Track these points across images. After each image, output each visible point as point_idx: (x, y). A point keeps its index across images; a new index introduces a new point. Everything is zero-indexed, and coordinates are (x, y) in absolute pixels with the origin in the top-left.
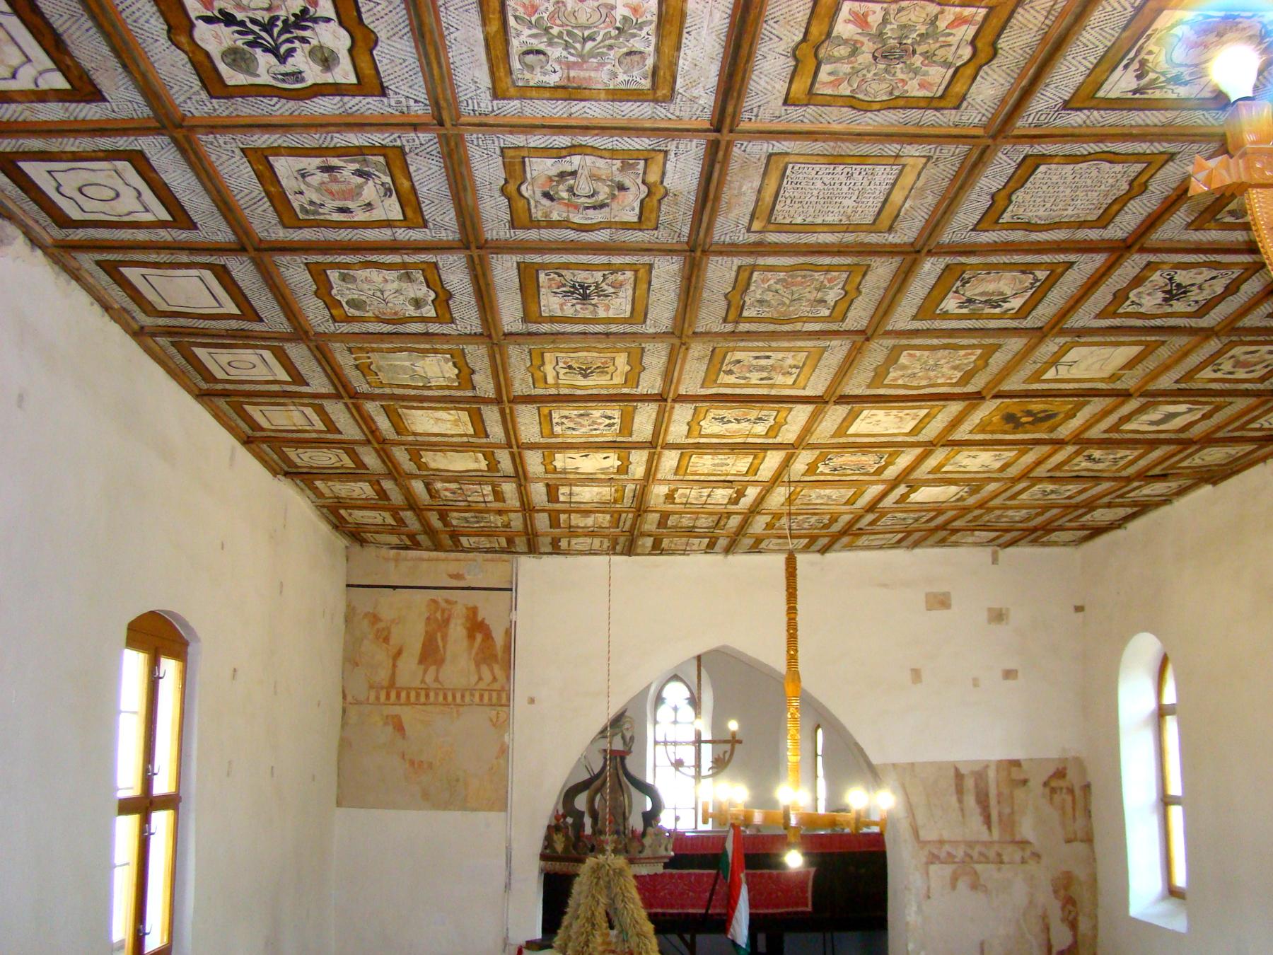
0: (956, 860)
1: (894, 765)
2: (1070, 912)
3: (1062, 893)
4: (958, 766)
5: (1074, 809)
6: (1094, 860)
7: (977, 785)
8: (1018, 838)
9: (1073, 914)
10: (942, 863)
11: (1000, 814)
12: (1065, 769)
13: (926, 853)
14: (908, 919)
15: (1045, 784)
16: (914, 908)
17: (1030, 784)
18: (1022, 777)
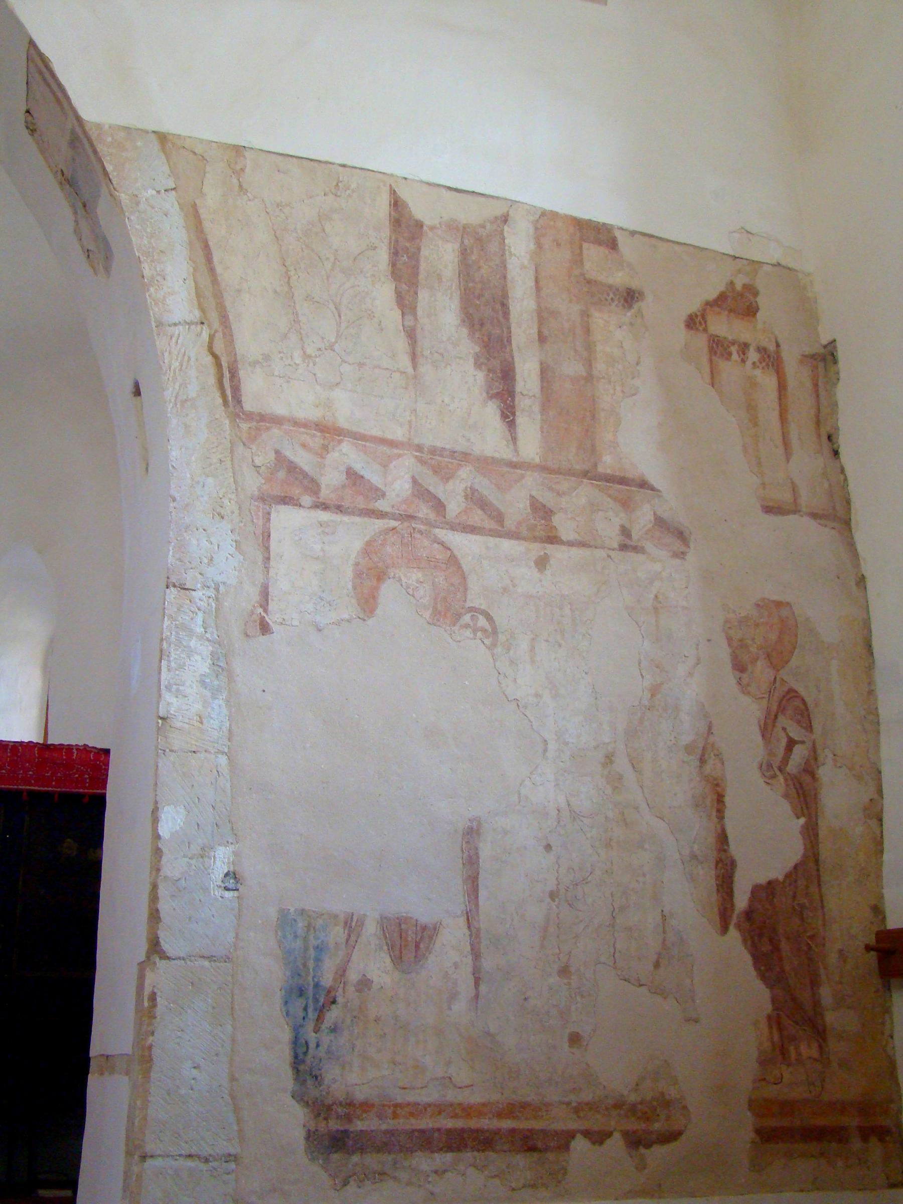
0: (382, 505)
1: (163, 138)
2: (791, 744)
3: (761, 671)
4: (404, 194)
5: (783, 419)
6: (861, 581)
7: (466, 268)
8: (607, 463)
9: (799, 753)
10: (324, 506)
11: (545, 372)
12: (751, 290)
13: (264, 458)
14: (171, 703)
15: (693, 322)
16: (201, 664)
17: (648, 305)
18: (619, 279)
